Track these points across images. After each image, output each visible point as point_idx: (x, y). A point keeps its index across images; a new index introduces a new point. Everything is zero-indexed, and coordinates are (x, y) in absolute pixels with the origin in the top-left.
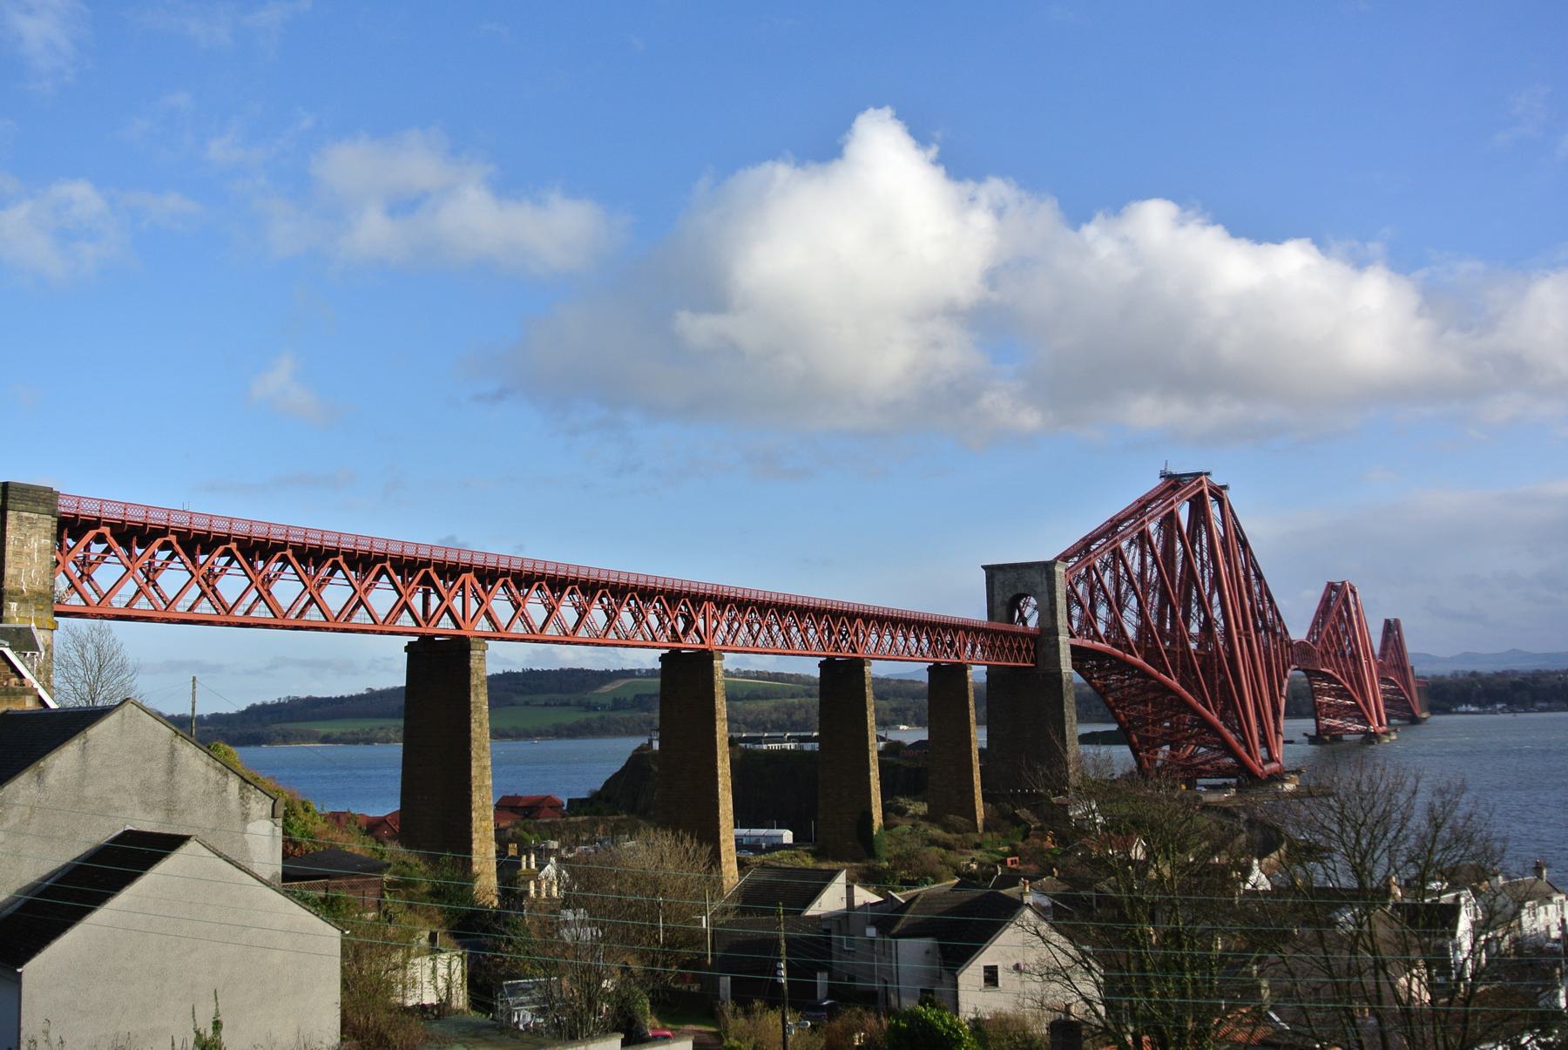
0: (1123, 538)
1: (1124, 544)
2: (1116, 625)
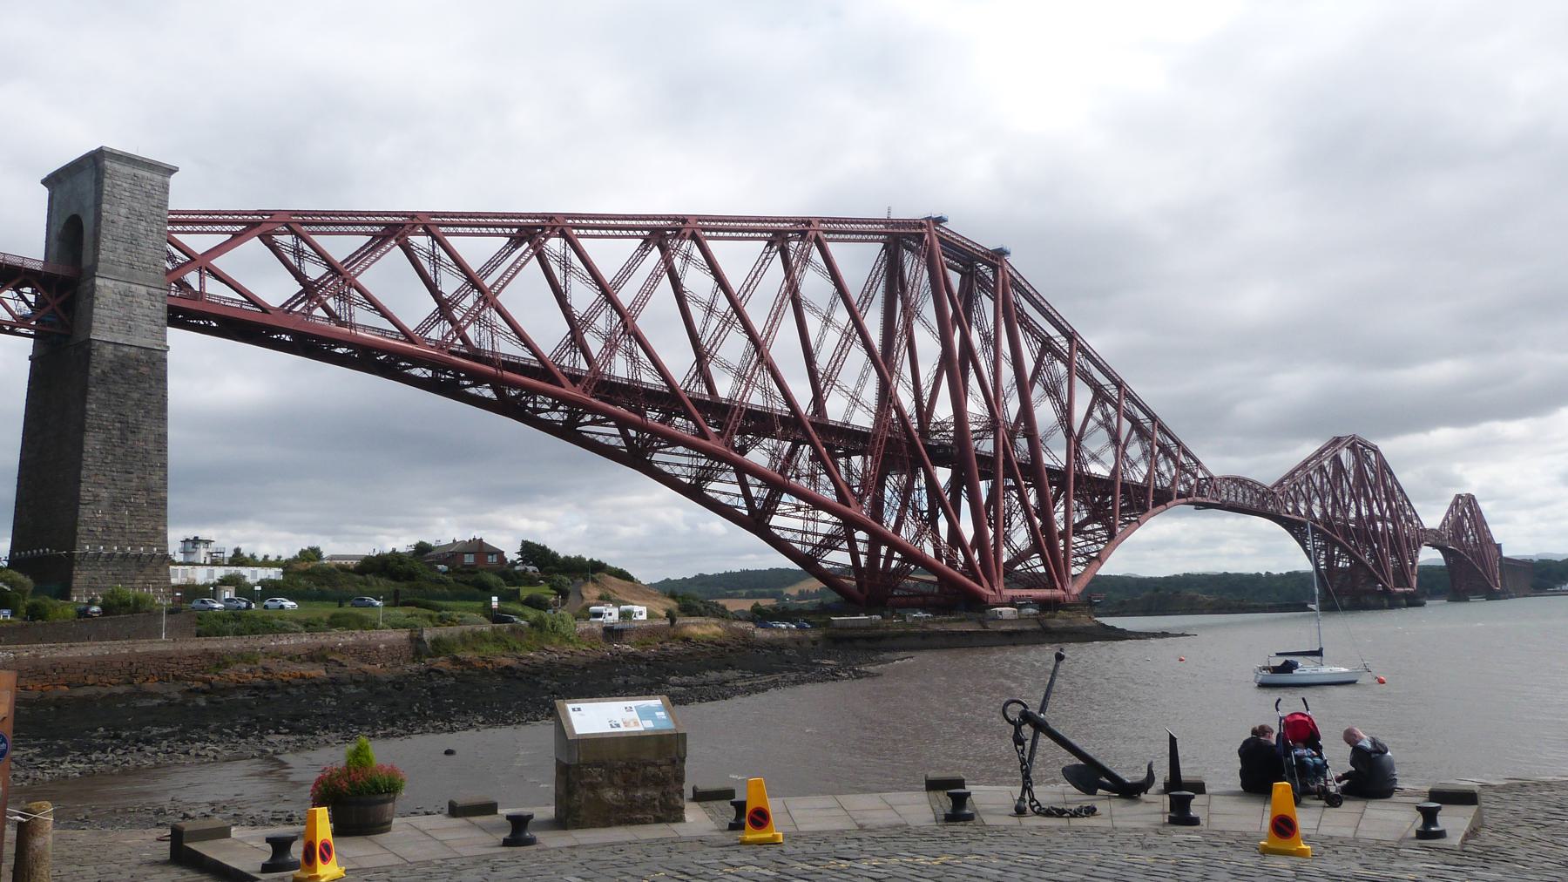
0: (1311, 469)
1: (1312, 472)
2: (1310, 512)
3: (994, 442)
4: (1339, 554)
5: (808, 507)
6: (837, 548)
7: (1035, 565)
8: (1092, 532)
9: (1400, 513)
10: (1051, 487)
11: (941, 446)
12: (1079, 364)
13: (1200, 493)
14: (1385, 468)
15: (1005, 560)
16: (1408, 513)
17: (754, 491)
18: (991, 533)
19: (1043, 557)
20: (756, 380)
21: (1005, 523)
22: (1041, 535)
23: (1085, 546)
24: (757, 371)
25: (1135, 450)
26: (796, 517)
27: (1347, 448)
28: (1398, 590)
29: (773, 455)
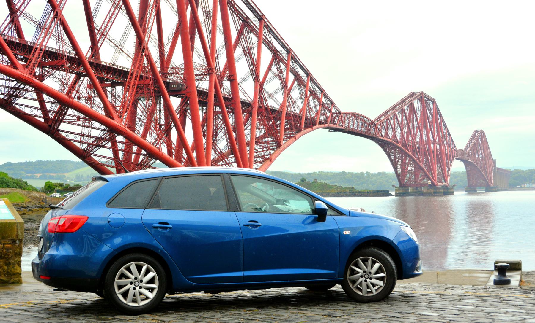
0: (397, 111)
2: (394, 136)
3: (209, 82)
4: (409, 162)
5: (85, 118)
6: (103, 146)
7: (231, 162)
8: (267, 142)
9: (444, 139)
10: (243, 113)
11: (175, 83)
12: (265, 36)
13: (333, 122)
14: (438, 113)
15: (212, 158)
16: (448, 140)
17: (48, 106)
18: (204, 141)
19: (236, 157)
20: (52, 30)
21: (213, 135)
22: (235, 143)
23: (262, 151)
24: (53, 25)
25: (295, 93)
26: (77, 125)
27: (418, 99)
28: (440, 184)
29: (62, 82)
